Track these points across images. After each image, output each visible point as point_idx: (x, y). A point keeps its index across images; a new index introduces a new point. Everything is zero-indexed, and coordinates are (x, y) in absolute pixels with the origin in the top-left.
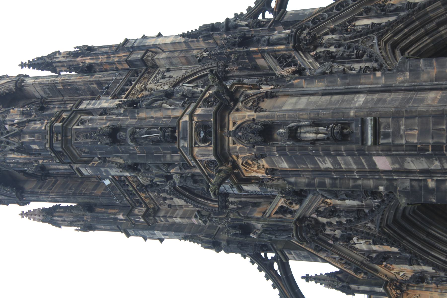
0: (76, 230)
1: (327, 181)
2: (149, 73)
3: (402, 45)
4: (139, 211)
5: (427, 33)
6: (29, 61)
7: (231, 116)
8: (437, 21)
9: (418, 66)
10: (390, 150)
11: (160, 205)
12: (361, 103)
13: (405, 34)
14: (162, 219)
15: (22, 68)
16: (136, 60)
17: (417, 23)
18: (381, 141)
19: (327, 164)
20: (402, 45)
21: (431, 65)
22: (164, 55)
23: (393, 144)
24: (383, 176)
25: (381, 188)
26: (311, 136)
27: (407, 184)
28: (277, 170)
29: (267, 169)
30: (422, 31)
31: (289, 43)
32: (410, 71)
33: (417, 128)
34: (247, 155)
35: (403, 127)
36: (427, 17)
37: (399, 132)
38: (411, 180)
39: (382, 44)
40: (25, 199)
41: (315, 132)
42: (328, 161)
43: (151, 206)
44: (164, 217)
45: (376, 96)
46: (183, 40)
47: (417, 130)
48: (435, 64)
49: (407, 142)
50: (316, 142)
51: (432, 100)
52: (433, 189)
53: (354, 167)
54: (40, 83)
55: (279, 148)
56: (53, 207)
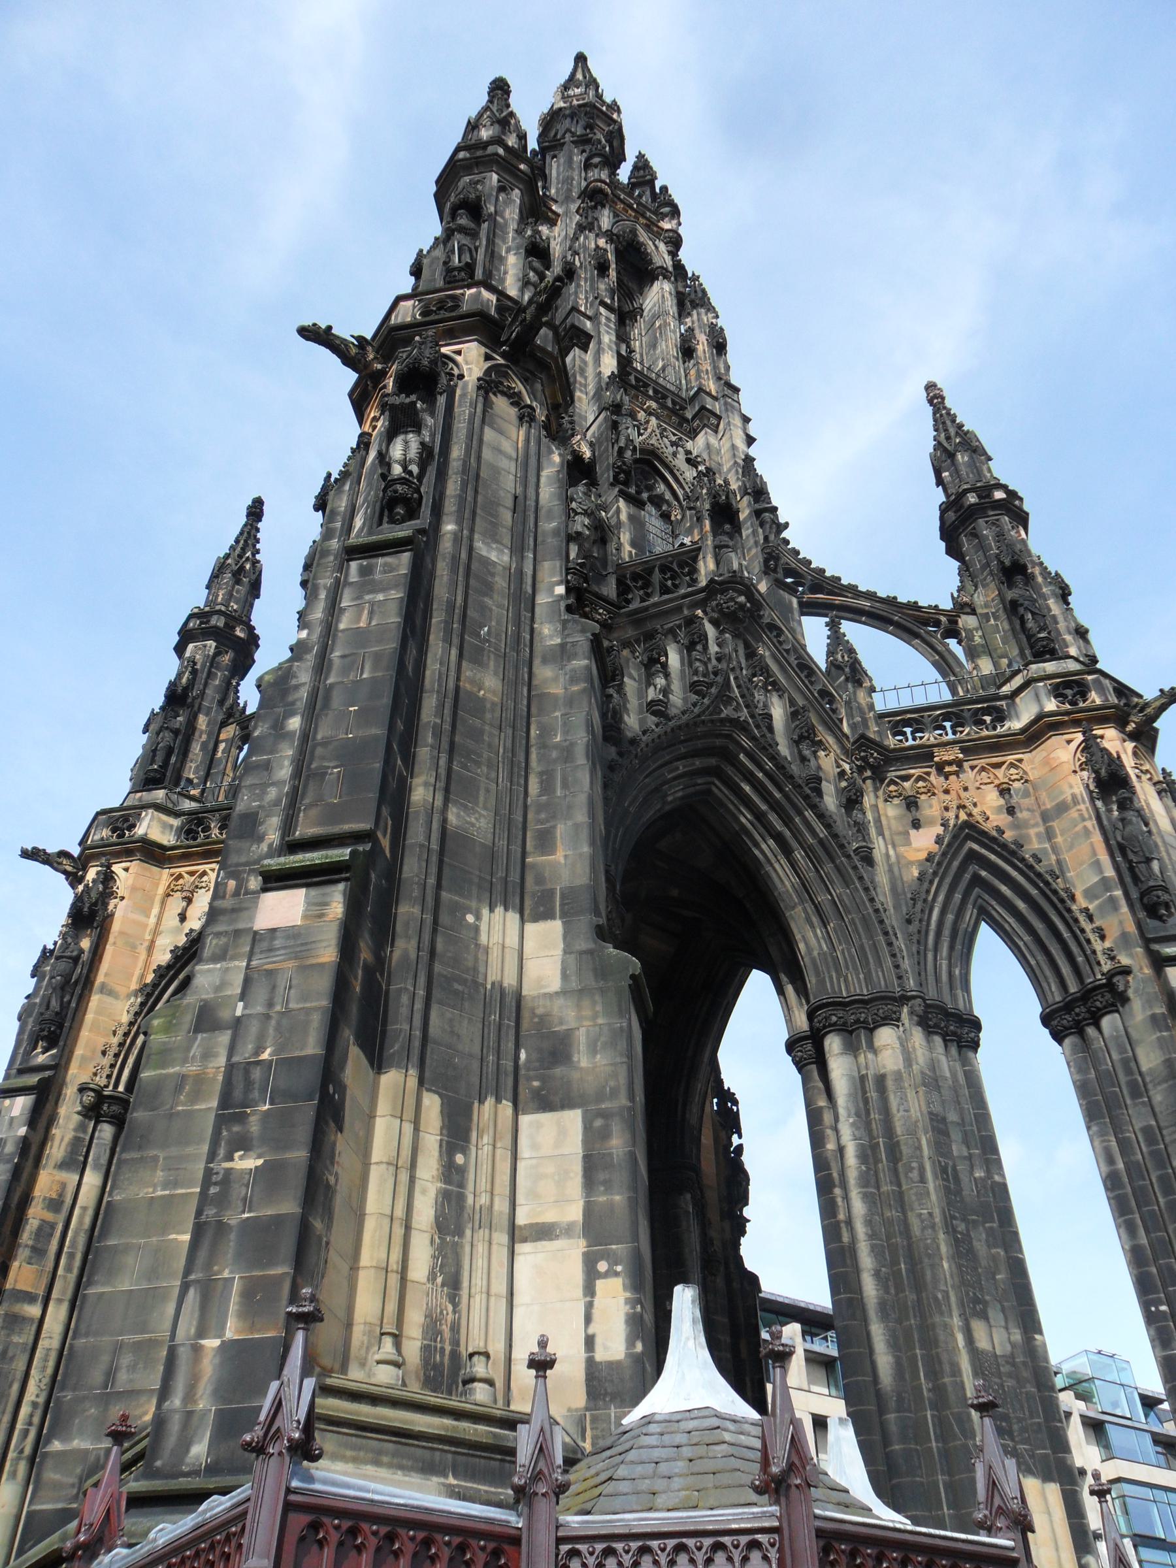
2: (680, 425)
3: (730, 771)
5: (760, 817)
8: (787, 833)
9: (574, 656)
12: (484, 553)
13: (752, 774)
17: (778, 795)
20: (730, 771)
21: (573, 680)
23: (344, 586)
30: (764, 807)
32: (563, 646)
33: (374, 623)
35: (380, 597)
36: (792, 813)
39: (726, 730)
48: (575, 688)
52: (282, 727)
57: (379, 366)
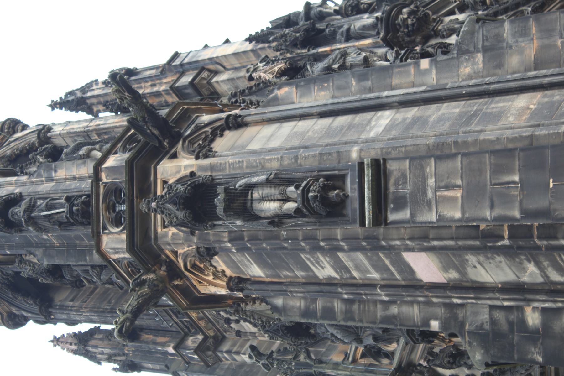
0: (114, 369)
1: (338, 306)
4: (193, 341)
6: (61, 98)
7: (160, 168)
9: (499, 38)
10: (425, 238)
11: (225, 332)
12: (381, 129)
14: (226, 355)
15: (53, 109)
16: (184, 87)
18: (392, 217)
19: (325, 270)
21: (524, 33)
22: (224, 77)
23: (414, 222)
24: (433, 297)
25: (435, 325)
26: (271, 207)
27: (484, 316)
28: (247, 280)
29: (231, 278)
31: (378, 33)
32: (485, 50)
33: (459, 182)
34: (186, 249)
35: (431, 182)
37: (425, 193)
38: (492, 307)
40: (52, 317)
41: (280, 197)
42: (327, 265)
43: (211, 333)
44: (229, 352)
45: (412, 113)
46: (249, 46)
47: (459, 186)
48: (534, 30)
49: (440, 218)
50: (284, 221)
51: (517, 112)
52: (536, 331)
53: (375, 275)
54: (69, 133)
55: (233, 235)
56: (91, 330)
57: (163, 268)
